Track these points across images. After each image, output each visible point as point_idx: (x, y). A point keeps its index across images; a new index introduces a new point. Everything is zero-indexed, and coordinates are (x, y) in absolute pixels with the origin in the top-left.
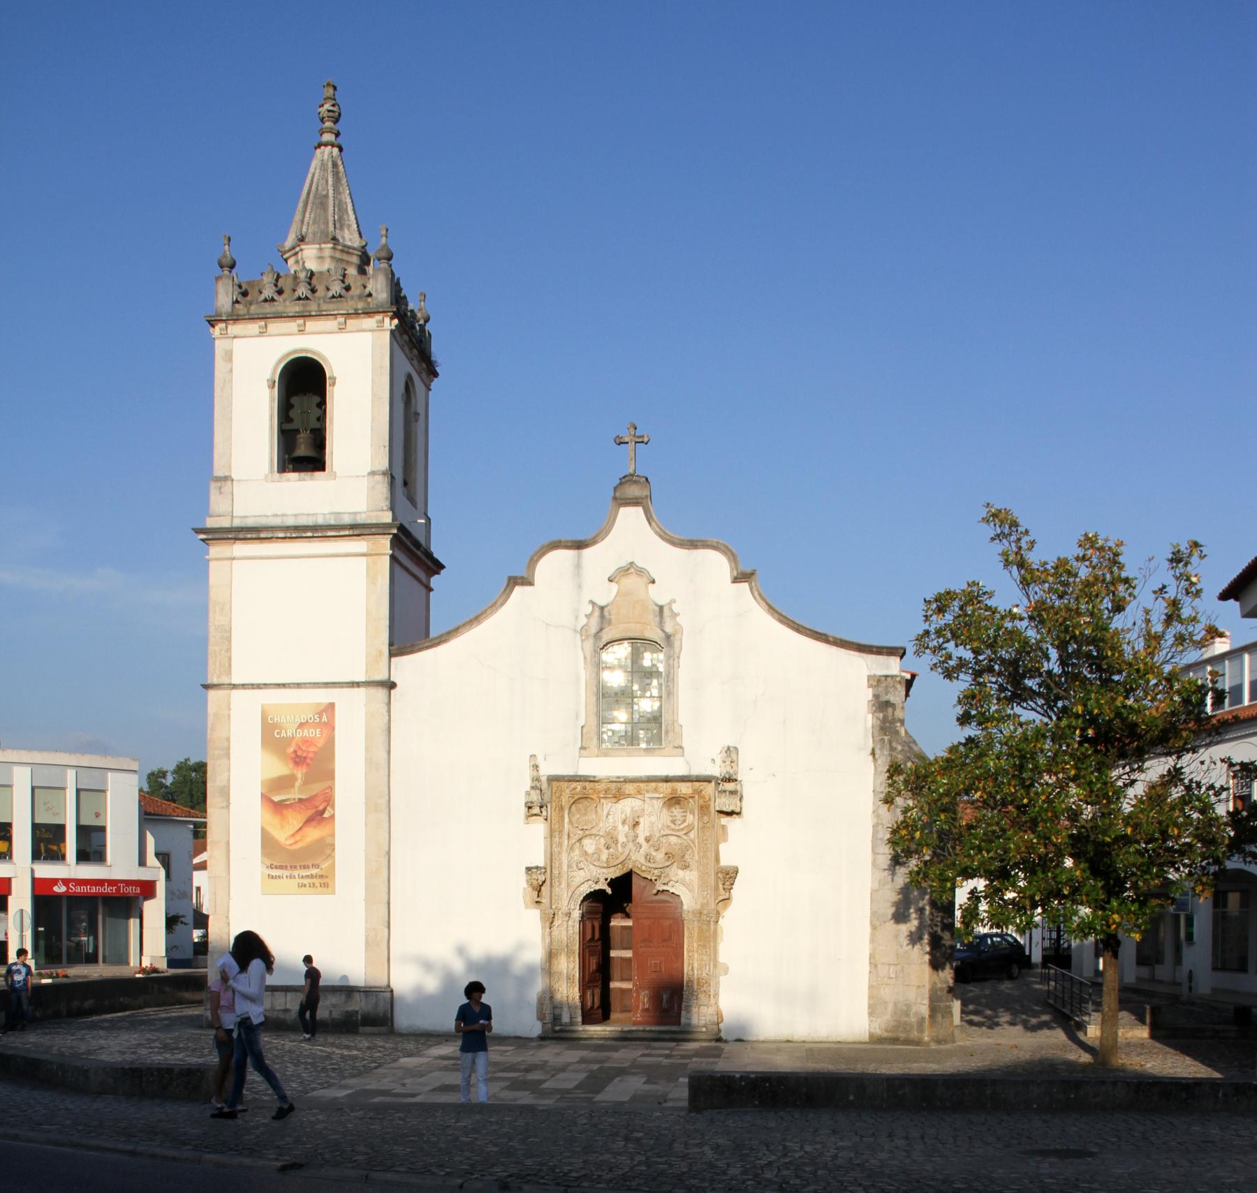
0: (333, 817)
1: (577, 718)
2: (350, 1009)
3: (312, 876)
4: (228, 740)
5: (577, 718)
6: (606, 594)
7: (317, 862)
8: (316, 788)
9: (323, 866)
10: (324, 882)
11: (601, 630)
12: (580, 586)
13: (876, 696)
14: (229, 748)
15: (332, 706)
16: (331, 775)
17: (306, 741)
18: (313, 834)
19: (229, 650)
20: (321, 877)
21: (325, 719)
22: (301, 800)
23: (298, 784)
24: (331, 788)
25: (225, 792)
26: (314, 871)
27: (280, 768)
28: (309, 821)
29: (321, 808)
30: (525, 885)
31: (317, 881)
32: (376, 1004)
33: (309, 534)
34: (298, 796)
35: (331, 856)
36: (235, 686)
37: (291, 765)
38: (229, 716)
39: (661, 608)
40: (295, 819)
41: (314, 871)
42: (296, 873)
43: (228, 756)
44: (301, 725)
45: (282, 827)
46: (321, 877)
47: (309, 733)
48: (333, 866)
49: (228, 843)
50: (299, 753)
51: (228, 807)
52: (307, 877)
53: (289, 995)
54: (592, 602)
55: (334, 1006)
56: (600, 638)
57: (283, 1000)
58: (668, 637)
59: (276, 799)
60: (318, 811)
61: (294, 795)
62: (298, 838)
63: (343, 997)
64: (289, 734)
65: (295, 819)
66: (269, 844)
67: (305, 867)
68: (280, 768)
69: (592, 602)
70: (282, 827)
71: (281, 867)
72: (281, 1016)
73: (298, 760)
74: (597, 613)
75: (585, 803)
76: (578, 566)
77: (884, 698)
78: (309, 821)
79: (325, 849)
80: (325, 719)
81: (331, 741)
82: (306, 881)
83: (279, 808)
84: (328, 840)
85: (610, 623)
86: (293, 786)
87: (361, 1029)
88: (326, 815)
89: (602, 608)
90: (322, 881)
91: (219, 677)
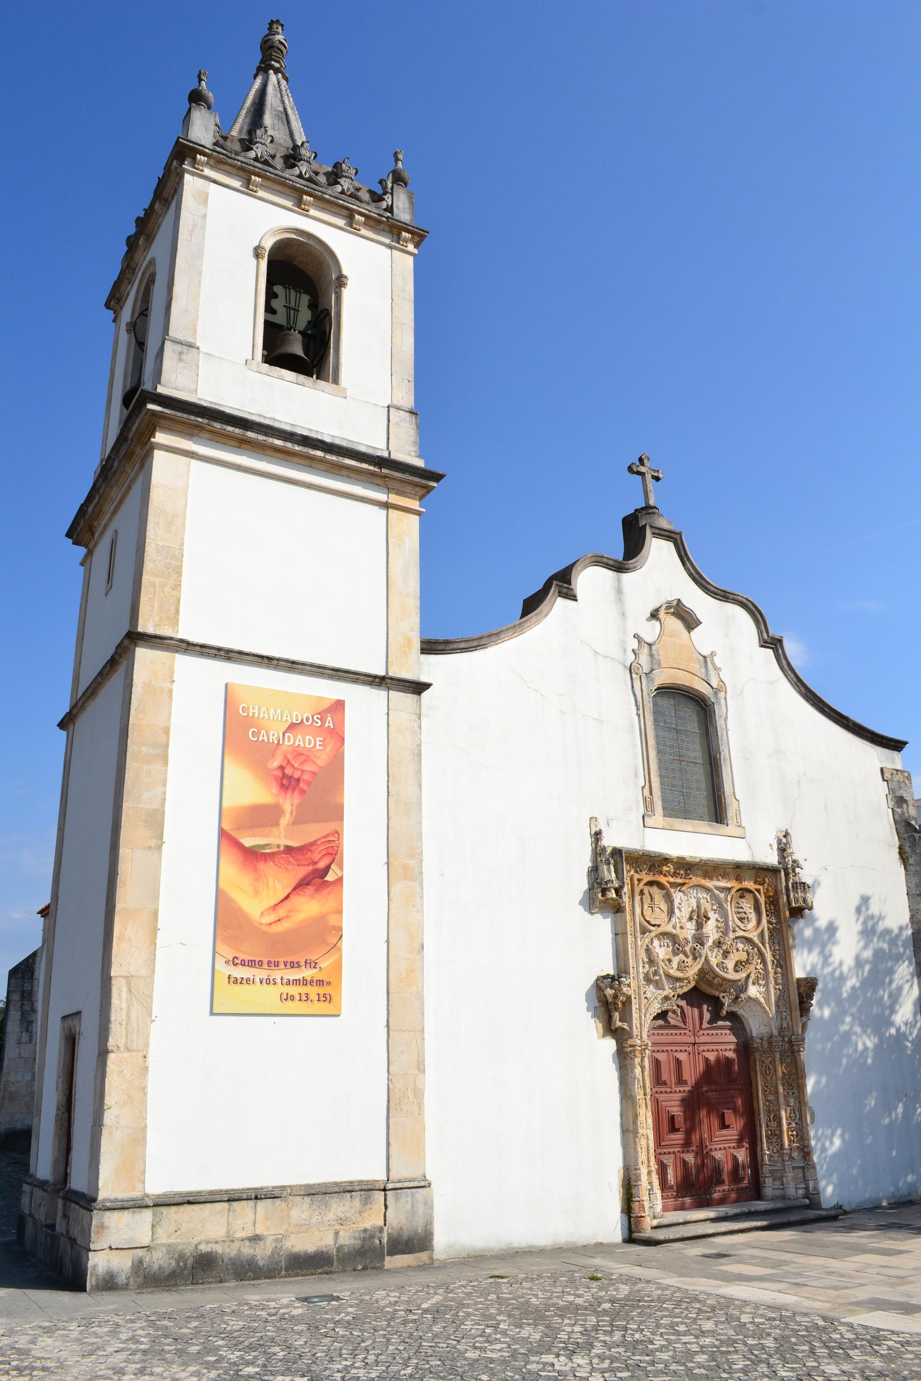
0: (340, 880)
1: (636, 775)
2: (368, 1225)
3: (304, 982)
4: (167, 731)
5: (636, 775)
6: (650, 632)
7: (312, 957)
8: (314, 832)
9: (323, 965)
10: (323, 996)
11: (652, 670)
12: (623, 615)
13: (891, 790)
14: (167, 745)
15: (339, 706)
16: (337, 813)
17: (298, 753)
18: (308, 907)
19: (177, 586)
20: (320, 983)
21: (329, 723)
22: (289, 850)
23: (285, 820)
24: (338, 834)
25: (156, 821)
26: (308, 973)
27: (250, 789)
28: (301, 885)
29: (322, 865)
30: (597, 1004)
31: (313, 991)
32: (413, 1213)
33: (319, 453)
34: (284, 842)
35: (335, 947)
36: (187, 647)
37: (275, 789)
38: (171, 692)
39: (705, 657)
40: (279, 880)
41: (308, 973)
42: (277, 974)
43: (164, 758)
44: (292, 727)
45: (257, 893)
46: (320, 983)
47: (305, 741)
48: (338, 967)
49: (155, 914)
50: (288, 771)
51: (159, 847)
52: (296, 982)
53: (261, 1204)
54: (636, 636)
55: (341, 1221)
56: (652, 680)
57: (250, 1218)
58: (716, 691)
59: (248, 842)
60: (317, 872)
61: (277, 838)
62: (282, 913)
63: (357, 1203)
64: (273, 738)
65: (279, 880)
66: (227, 919)
67: (294, 965)
68: (250, 789)
69: (636, 636)
70: (257, 893)
71: (251, 964)
72: (247, 1250)
73: (287, 782)
74: (646, 649)
75: (655, 890)
76: (619, 591)
77: (898, 794)
78: (301, 885)
79: (327, 934)
80: (329, 723)
81: (338, 760)
82: (294, 990)
83: (253, 857)
84: (332, 920)
85: (660, 666)
86: (277, 824)
87: (390, 1262)
88: (330, 877)
89: (650, 645)
90: (322, 990)
91: (157, 625)
